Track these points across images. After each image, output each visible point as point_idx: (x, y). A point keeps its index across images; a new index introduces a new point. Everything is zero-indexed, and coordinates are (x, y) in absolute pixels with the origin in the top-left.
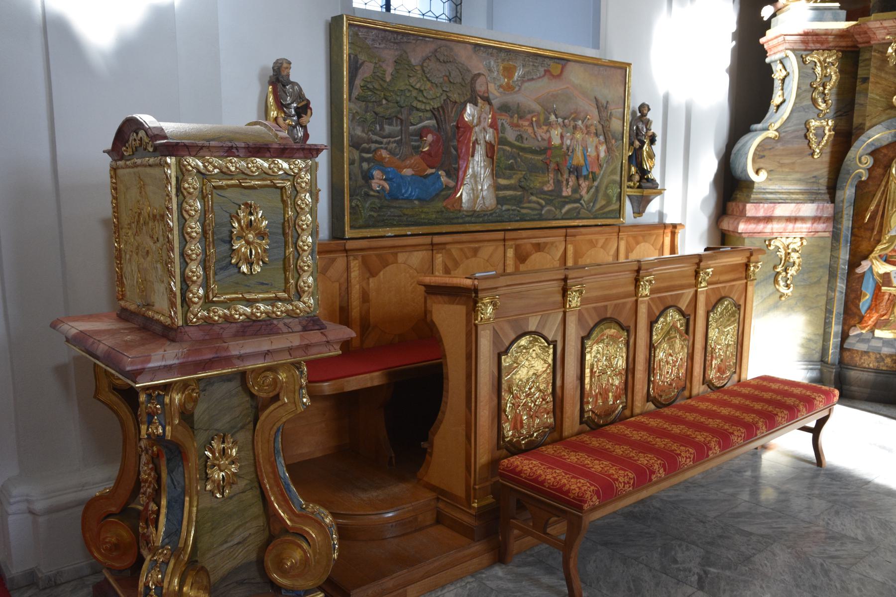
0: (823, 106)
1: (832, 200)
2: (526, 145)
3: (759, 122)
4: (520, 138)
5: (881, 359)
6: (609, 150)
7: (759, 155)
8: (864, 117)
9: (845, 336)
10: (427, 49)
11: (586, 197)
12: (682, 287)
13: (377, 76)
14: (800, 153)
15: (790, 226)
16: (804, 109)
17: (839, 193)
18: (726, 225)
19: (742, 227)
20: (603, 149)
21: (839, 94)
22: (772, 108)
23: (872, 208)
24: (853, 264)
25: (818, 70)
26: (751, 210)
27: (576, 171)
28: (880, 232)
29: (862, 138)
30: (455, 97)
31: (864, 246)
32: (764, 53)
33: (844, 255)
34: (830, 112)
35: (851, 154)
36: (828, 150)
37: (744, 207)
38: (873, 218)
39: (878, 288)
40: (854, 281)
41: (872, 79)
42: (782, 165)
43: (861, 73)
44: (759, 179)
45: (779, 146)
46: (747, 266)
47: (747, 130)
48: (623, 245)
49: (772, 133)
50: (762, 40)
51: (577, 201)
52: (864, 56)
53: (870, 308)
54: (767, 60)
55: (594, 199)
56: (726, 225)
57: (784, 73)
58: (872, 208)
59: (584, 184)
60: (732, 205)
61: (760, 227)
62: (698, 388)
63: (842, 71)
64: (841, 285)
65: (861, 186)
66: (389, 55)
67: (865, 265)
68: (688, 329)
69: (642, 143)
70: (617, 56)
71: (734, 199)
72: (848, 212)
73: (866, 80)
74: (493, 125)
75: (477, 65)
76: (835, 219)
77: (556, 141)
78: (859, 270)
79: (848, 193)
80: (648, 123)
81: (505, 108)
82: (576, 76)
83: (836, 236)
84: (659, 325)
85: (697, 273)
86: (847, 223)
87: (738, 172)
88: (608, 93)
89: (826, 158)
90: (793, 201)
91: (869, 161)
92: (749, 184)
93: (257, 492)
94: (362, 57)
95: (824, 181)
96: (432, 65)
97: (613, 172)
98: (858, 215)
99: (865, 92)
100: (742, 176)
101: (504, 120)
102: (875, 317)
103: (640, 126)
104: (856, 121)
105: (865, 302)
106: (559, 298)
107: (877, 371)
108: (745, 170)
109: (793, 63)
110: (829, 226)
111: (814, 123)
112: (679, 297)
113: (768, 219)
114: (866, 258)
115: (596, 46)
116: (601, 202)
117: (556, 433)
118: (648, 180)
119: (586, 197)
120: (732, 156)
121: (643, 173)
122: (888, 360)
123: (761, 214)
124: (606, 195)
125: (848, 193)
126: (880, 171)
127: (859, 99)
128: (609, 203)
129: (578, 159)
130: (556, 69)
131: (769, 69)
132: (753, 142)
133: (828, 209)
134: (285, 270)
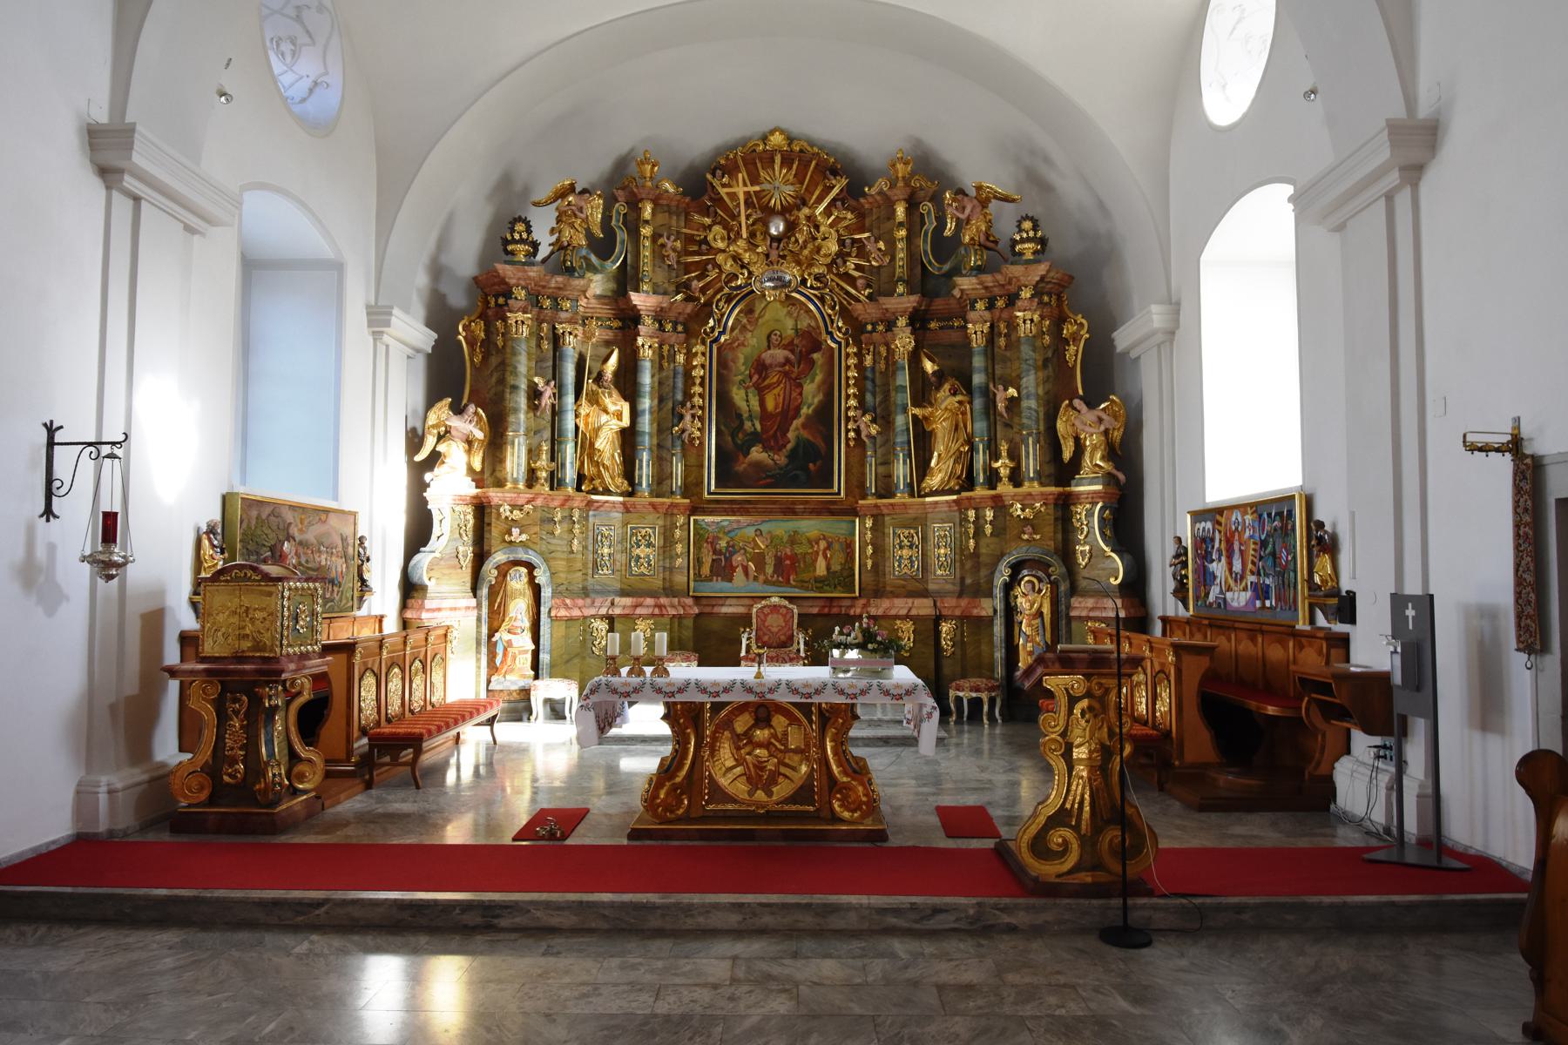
0: (466, 538)
1: (475, 596)
2: (309, 565)
3: (425, 546)
4: (307, 562)
5: (510, 693)
6: (347, 567)
7: (430, 569)
8: (490, 546)
9: (489, 682)
10: (267, 511)
11: (337, 598)
12: (421, 647)
13: (249, 527)
14: (454, 567)
15: (453, 613)
16: (455, 540)
17: (478, 592)
18: (409, 614)
19: (424, 615)
20: (344, 566)
21: (474, 531)
22: (434, 537)
23: (498, 600)
24: (491, 635)
25: (462, 516)
26: (428, 604)
27: (332, 582)
28: (504, 615)
29: (490, 558)
30: (281, 537)
31: (496, 624)
32: (425, 502)
33: (485, 630)
34: (470, 542)
35: (484, 568)
36: (470, 565)
37: (423, 602)
38: (499, 606)
39: (505, 649)
40: (492, 647)
41: (493, 525)
42: (444, 574)
43: (486, 520)
44: (431, 585)
45: (442, 562)
46: (446, 635)
47: (418, 552)
48: (355, 628)
49: (437, 555)
50: (425, 494)
51: (332, 601)
52: (488, 510)
53: (502, 662)
54: (429, 507)
55: (341, 600)
56: (409, 614)
57: (441, 517)
58: (498, 600)
59: (336, 589)
60: (411, 602)
61: (435, 614)
62: (429, 708)
63: (475, 517)
64: (484, 650)
65: (491, 587)
66: (254, 513)
67: (497, 635)
68: (424, 667)
69: (363, 561)
70: (346, 508)
71: (413, 597)
72: (485, 604)
73: (489, 524)
74: (296, 554)
75: (289, 516)
76: (479, 606)
77: (323, 563)
78: (494, 639)
79: (484, 591)
80: (364, 549)
81: (301, 543)
82: (333, 521)
83: (479, 619)
84: (413, 668)
85: (427, 639)
86: (485, 610)
87: (415, 578)
88: (348, 531)
89: (469, 570)
90: (454, 598)
91: (495, 573)
92: (423, 588)
93: (286, 742)
94: (244, 516)
95: (468, 585)
96: (272, 518)
97: (349, 582)
98: (491, 605)
99: (490, 531)
100: (419, 582)
101: (301, 550)
102: (506, 667)
103: (361, 550)
104: (486, 548)
105: (498, 661)
106: (378, 650)
107: (509, 702)
108: (421, 578)
109: (447, 513)
110: (475, 613)
111: (461, 549)
112: (419, 652)
113: (439, 610)
114: (497, 631)
115: (336, 498)
116: (344, 602)
117: (378, 723)
118: (367, 586)
119: (337, 598)
120: (410, 569)
121: (363, 582)
122: (514, 694)
123: (434, 606)
124: (347, 598)
125: (484, 591)
126: (501, 578)
127: (486, 535)
128: (348, 602)
129: (333, 575)
130: (323, 517)
131: (429, 513)
132: (423, 559)
133: (473, 602)
134: (313, 631)
